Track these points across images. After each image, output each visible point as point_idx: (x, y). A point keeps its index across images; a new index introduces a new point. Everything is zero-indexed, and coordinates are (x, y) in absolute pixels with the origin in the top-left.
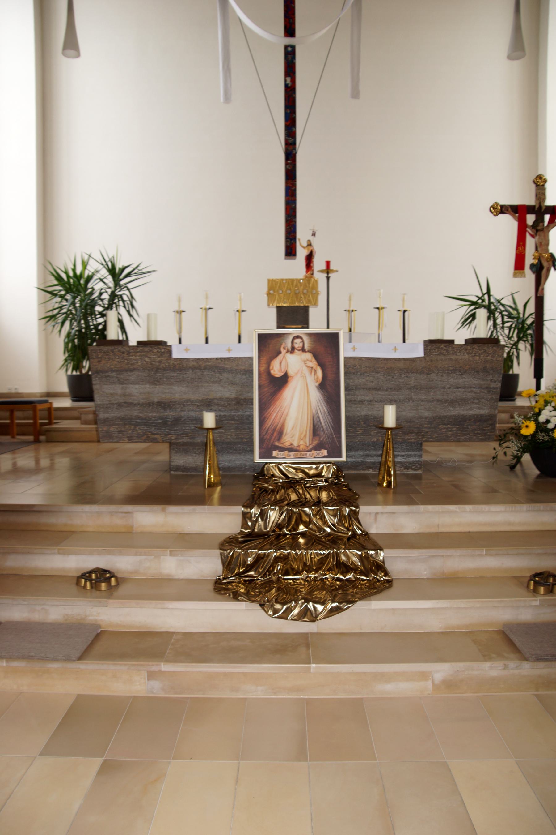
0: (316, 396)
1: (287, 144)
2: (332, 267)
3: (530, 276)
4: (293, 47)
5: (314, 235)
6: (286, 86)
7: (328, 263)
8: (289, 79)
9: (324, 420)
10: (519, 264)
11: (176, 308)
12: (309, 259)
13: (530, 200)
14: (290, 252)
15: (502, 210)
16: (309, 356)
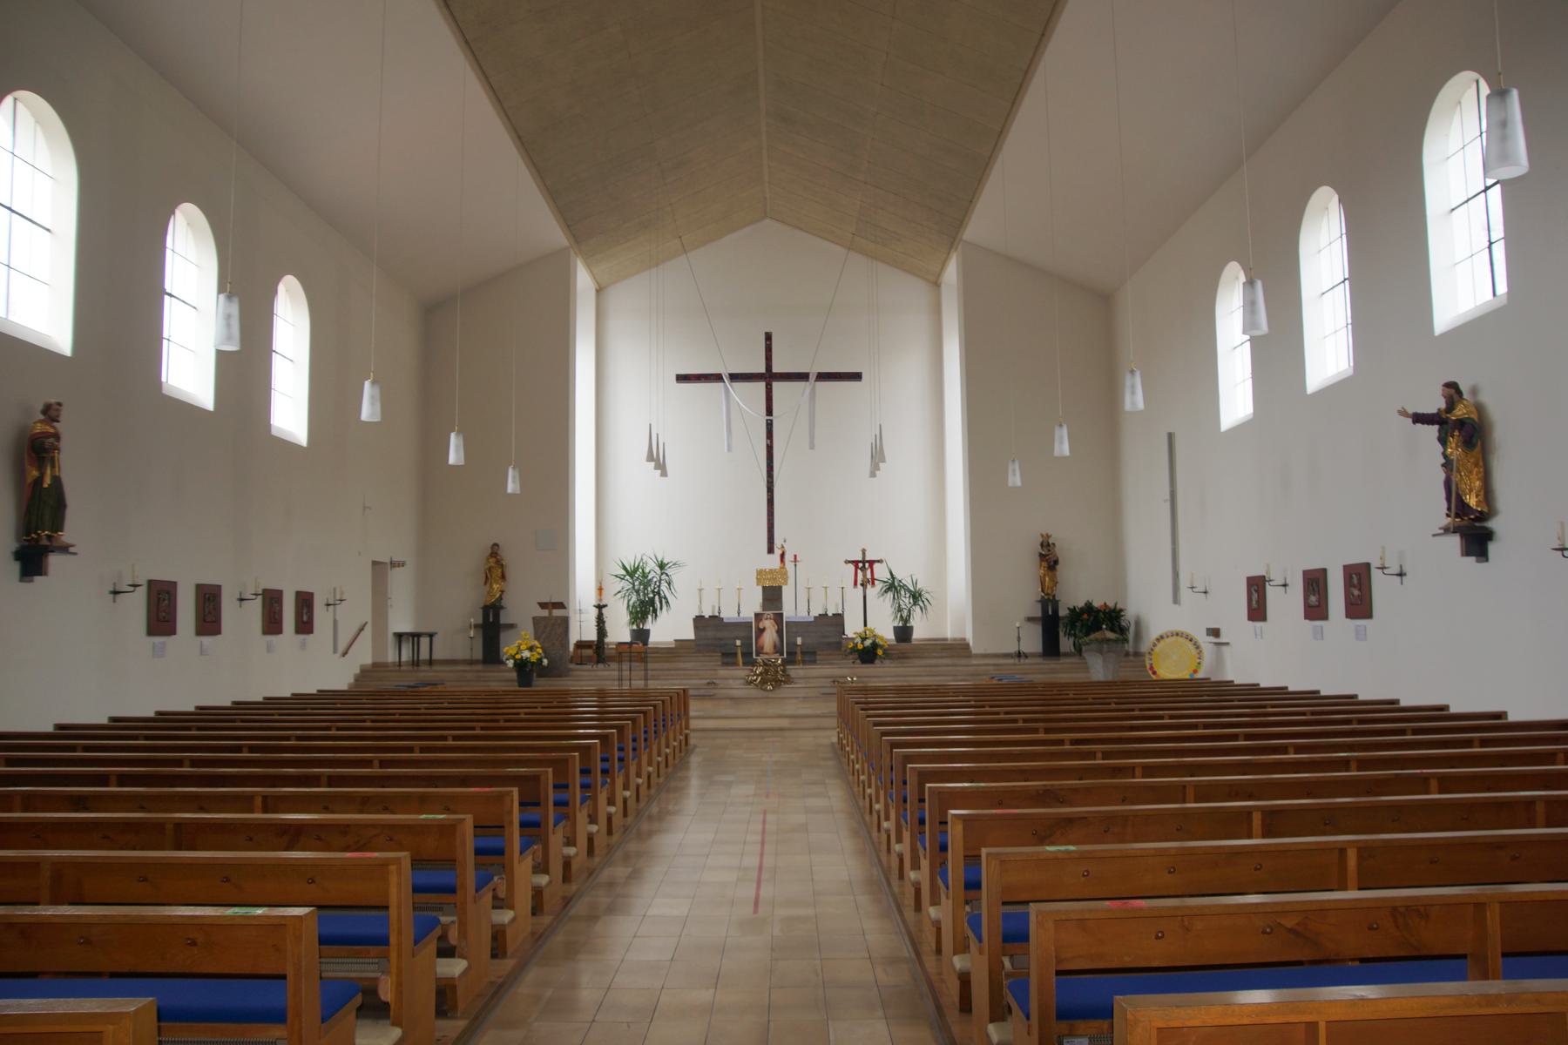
0: (775, 635)
1: (768, 482)
2: (798, 559)
3: (860, 588)
4: (771, 420)
5: (785, 541)
6: (767, 445)
7: (795, 556)
8: (769, 441)
9: (778, 643)
10: (856, 584)
11: (699, 587)
12: (782, 556)
13: (860, 559)
14: (771, 550)
15: (847, 562)
16: (772, 621)
